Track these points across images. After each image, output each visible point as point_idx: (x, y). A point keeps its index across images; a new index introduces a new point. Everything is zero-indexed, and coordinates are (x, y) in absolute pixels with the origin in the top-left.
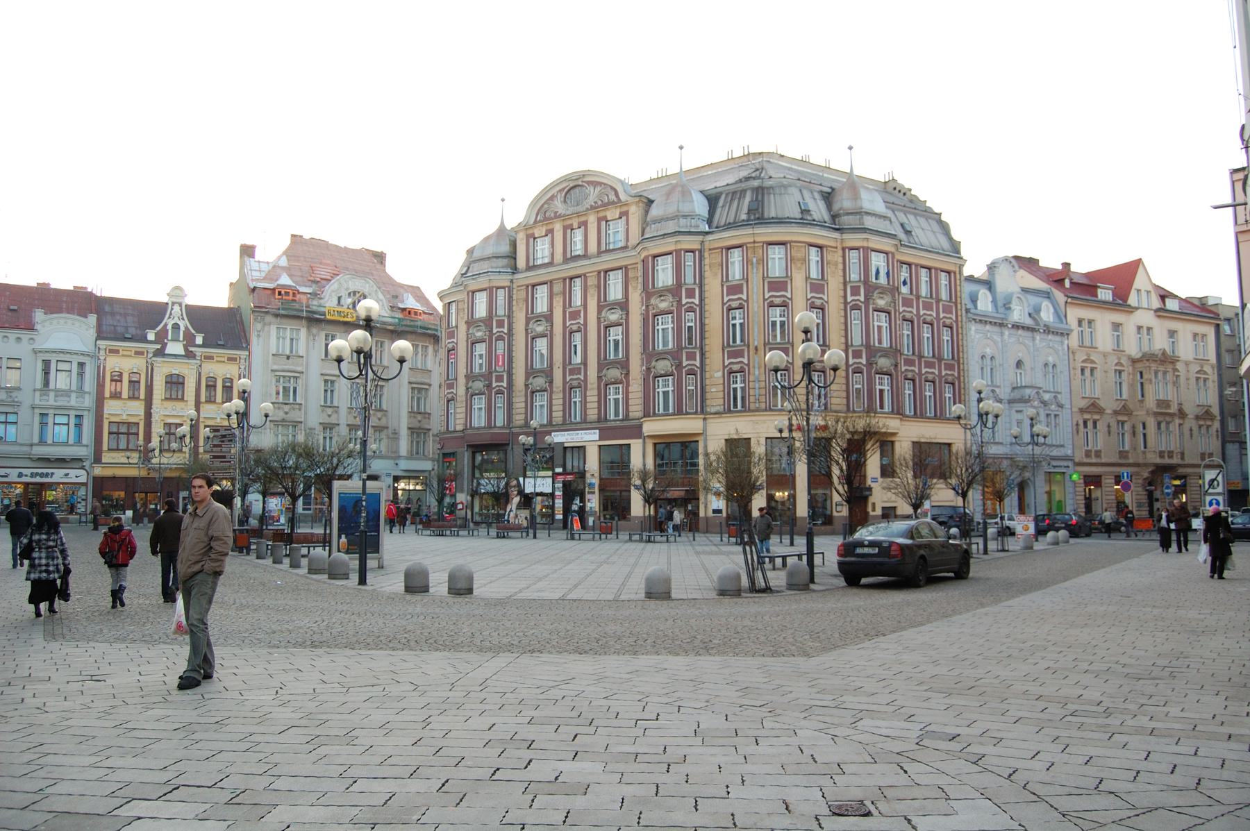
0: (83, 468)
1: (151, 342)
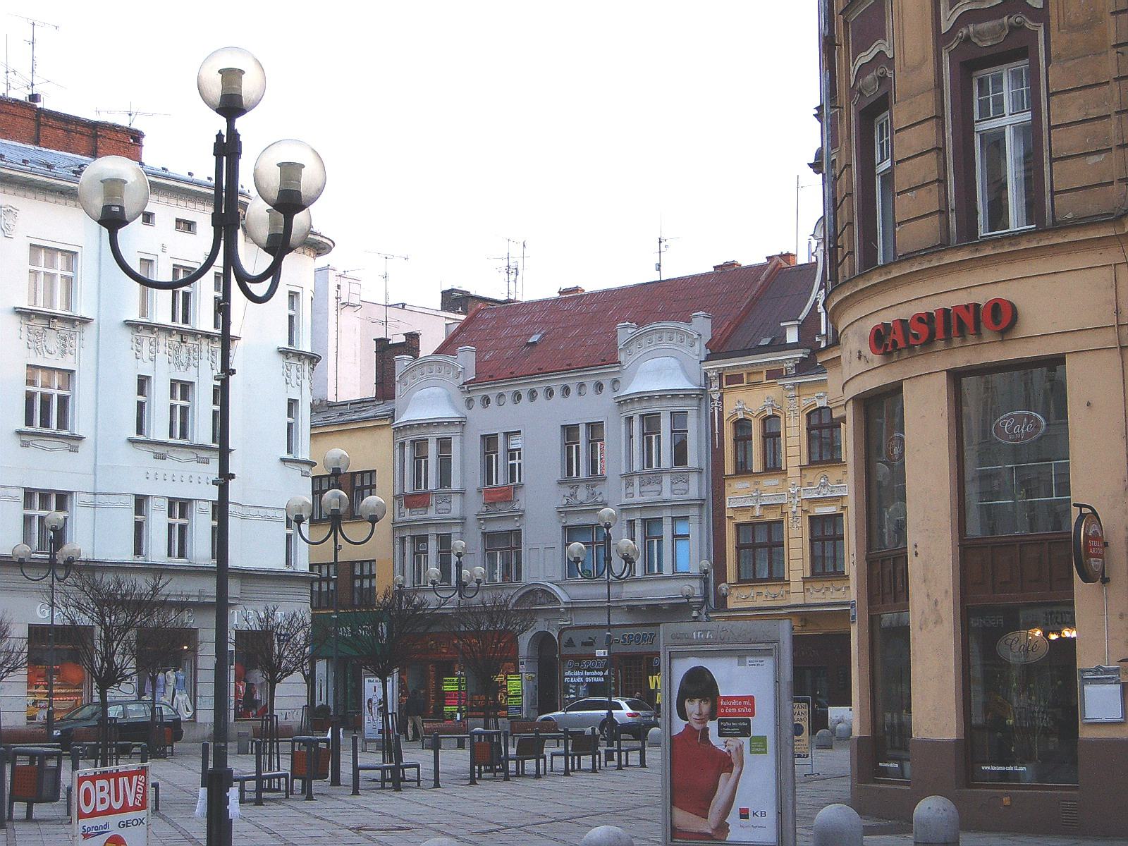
1: (793, 346)
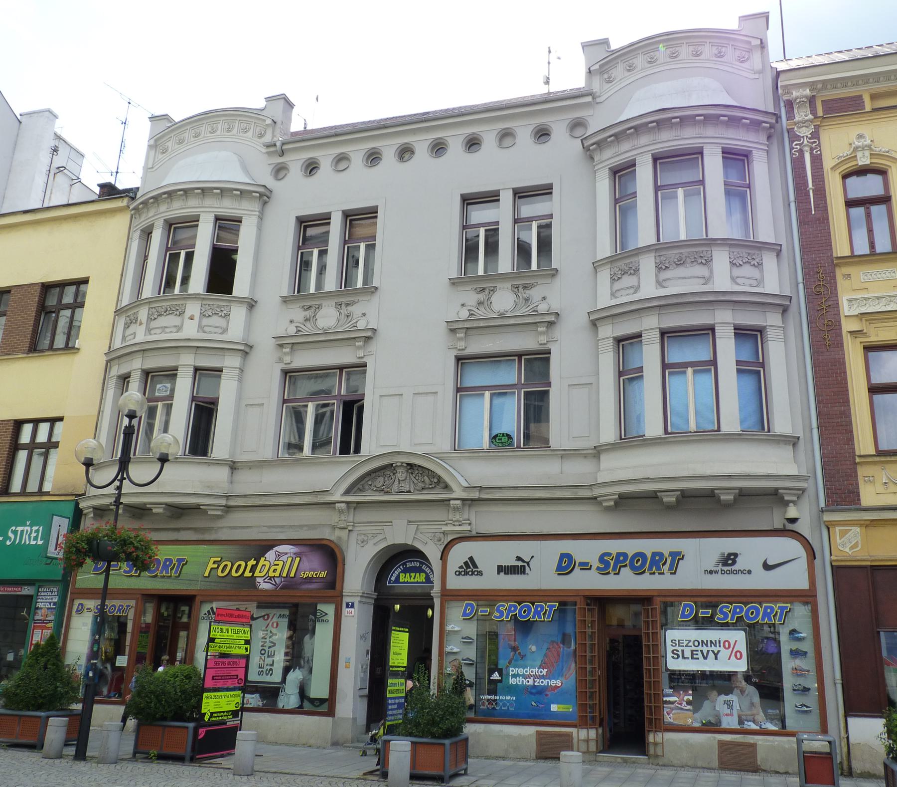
0: (787, 530)
